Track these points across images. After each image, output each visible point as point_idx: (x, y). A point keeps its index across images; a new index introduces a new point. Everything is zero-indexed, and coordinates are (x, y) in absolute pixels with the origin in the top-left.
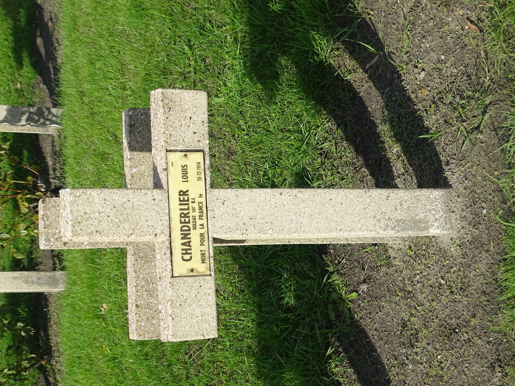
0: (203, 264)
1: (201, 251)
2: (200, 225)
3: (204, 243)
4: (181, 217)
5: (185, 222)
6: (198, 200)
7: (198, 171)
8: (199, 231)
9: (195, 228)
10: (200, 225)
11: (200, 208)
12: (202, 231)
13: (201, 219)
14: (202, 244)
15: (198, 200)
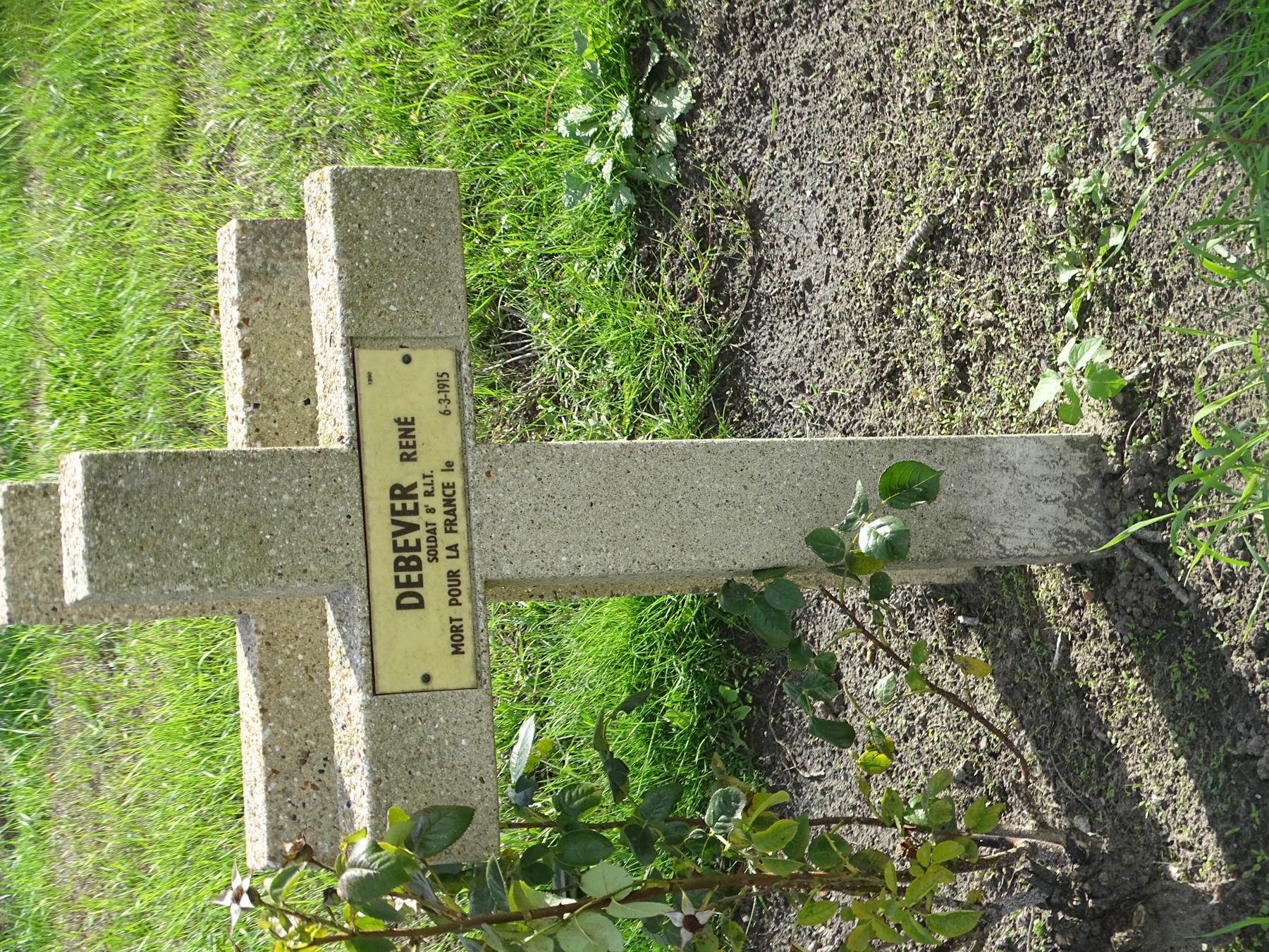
0: (456, 656)
1: (451, 620)
2: (449, 548)
3: (460, 599)
4: (397, 568)
5: (409, 583)
6: (440, 478)
7: (442, 396)
8: (445, 565)
9: (434, 557)
10: (449, 548)
11: (449, 502)
12: (454, 565)
13: (451, 531)
14: (454, 602)
15: (440, 478)
